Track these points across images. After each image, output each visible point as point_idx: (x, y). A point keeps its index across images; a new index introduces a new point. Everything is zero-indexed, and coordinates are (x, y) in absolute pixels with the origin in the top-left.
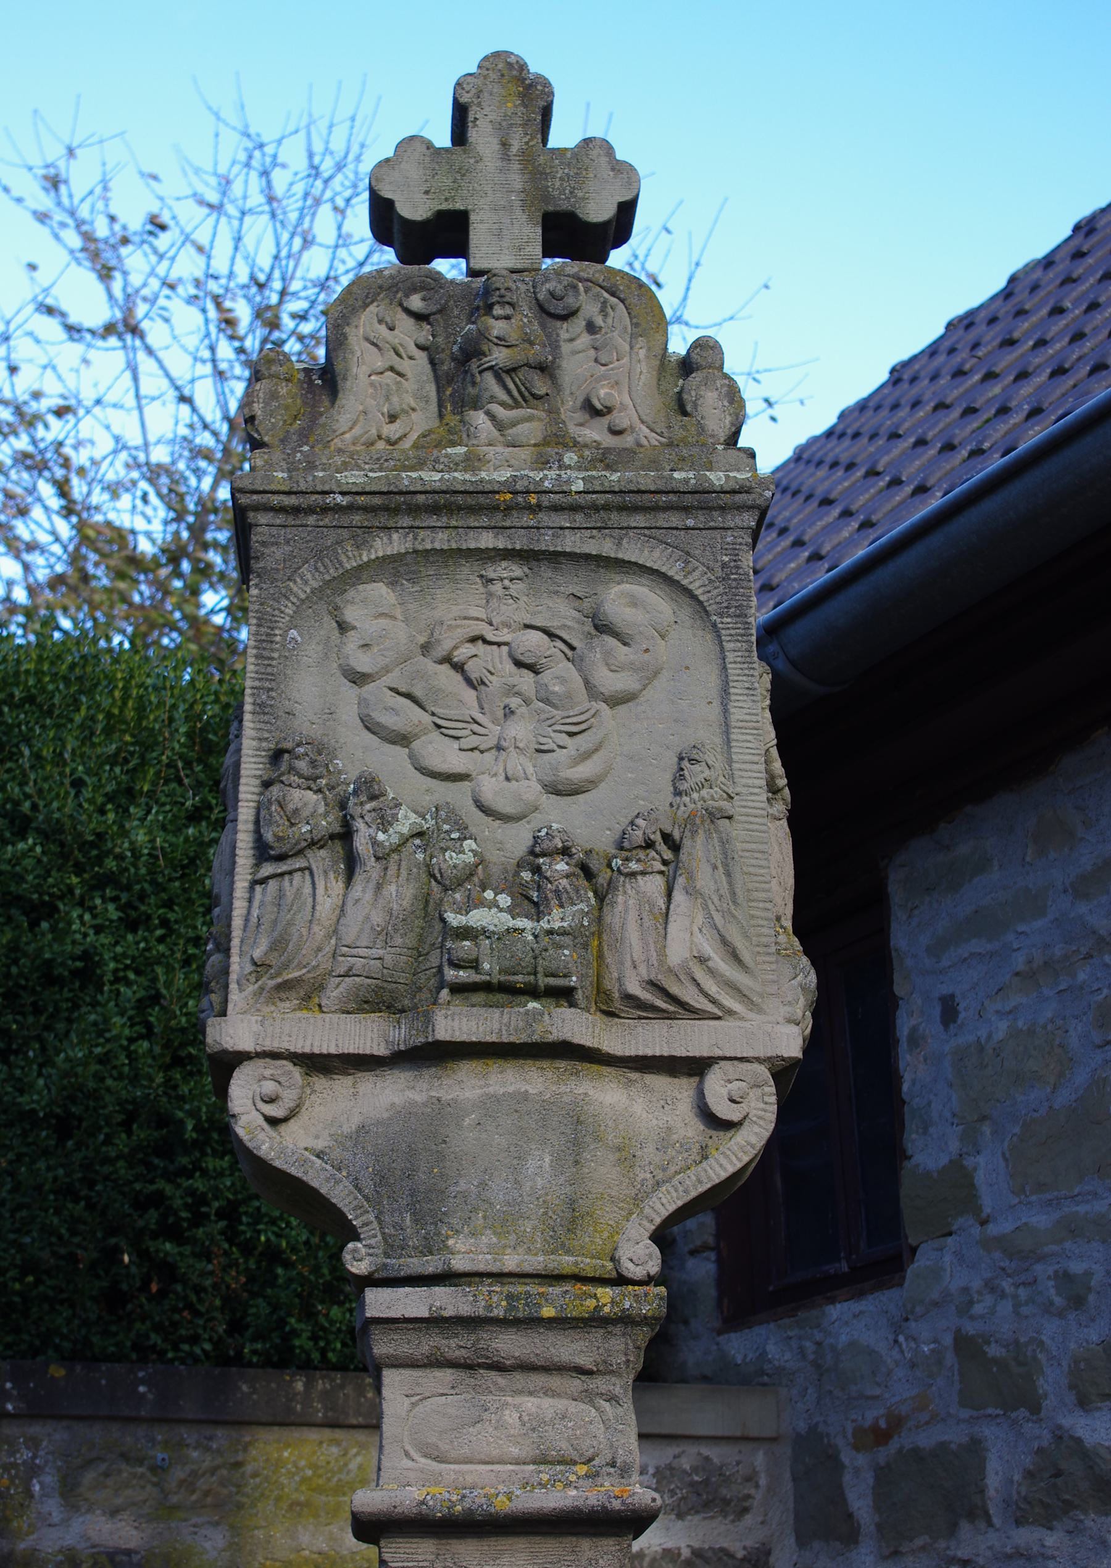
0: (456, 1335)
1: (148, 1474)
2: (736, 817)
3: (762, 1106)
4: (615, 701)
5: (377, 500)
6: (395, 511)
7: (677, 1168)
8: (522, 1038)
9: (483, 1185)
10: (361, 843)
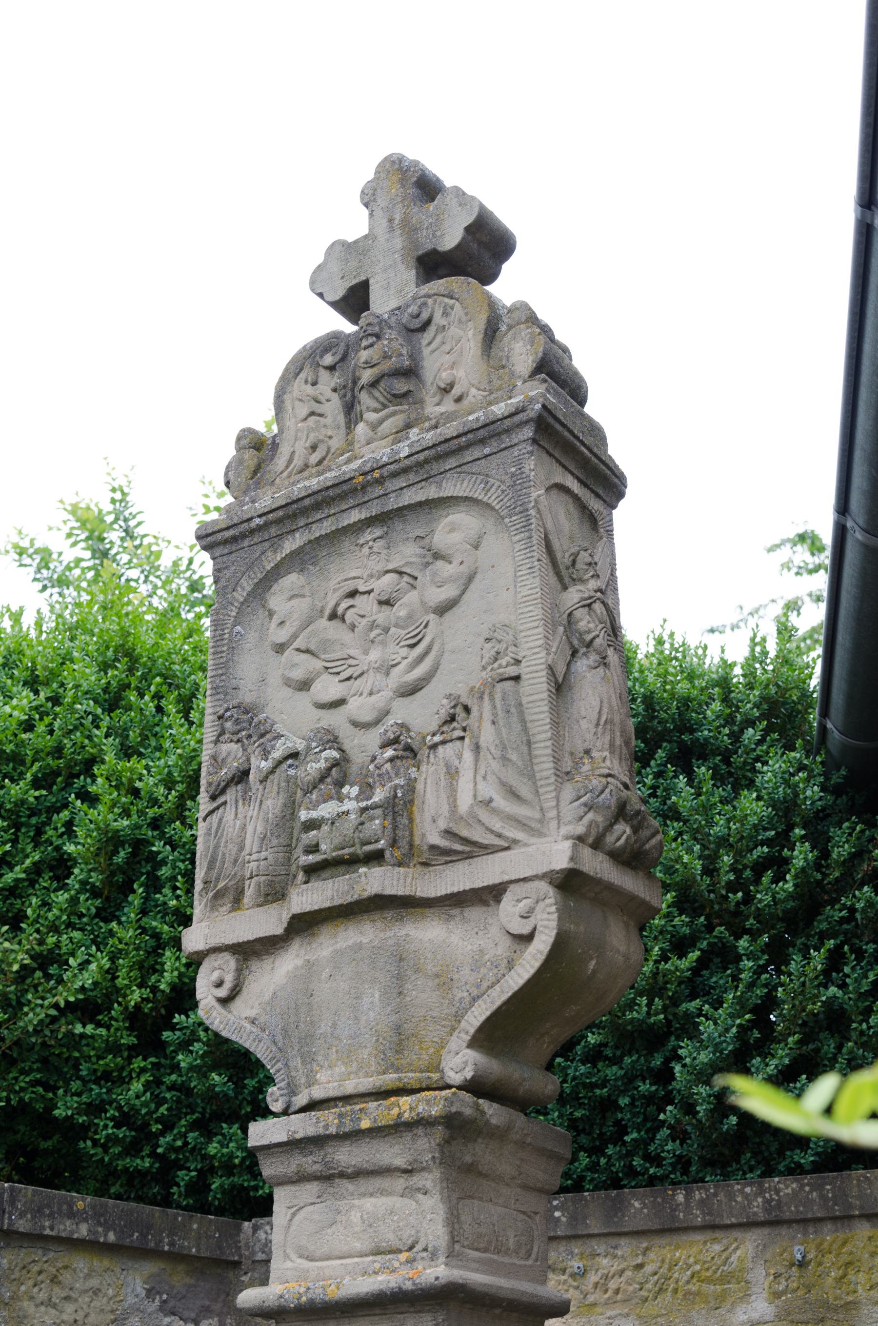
0: (311, 1153)
1: (570, 1280)
2: (524, 677)
3: (546, 916)
5: (280, 513)
6: (294, 516)
7: (489, 983)
9: (334, 1026)
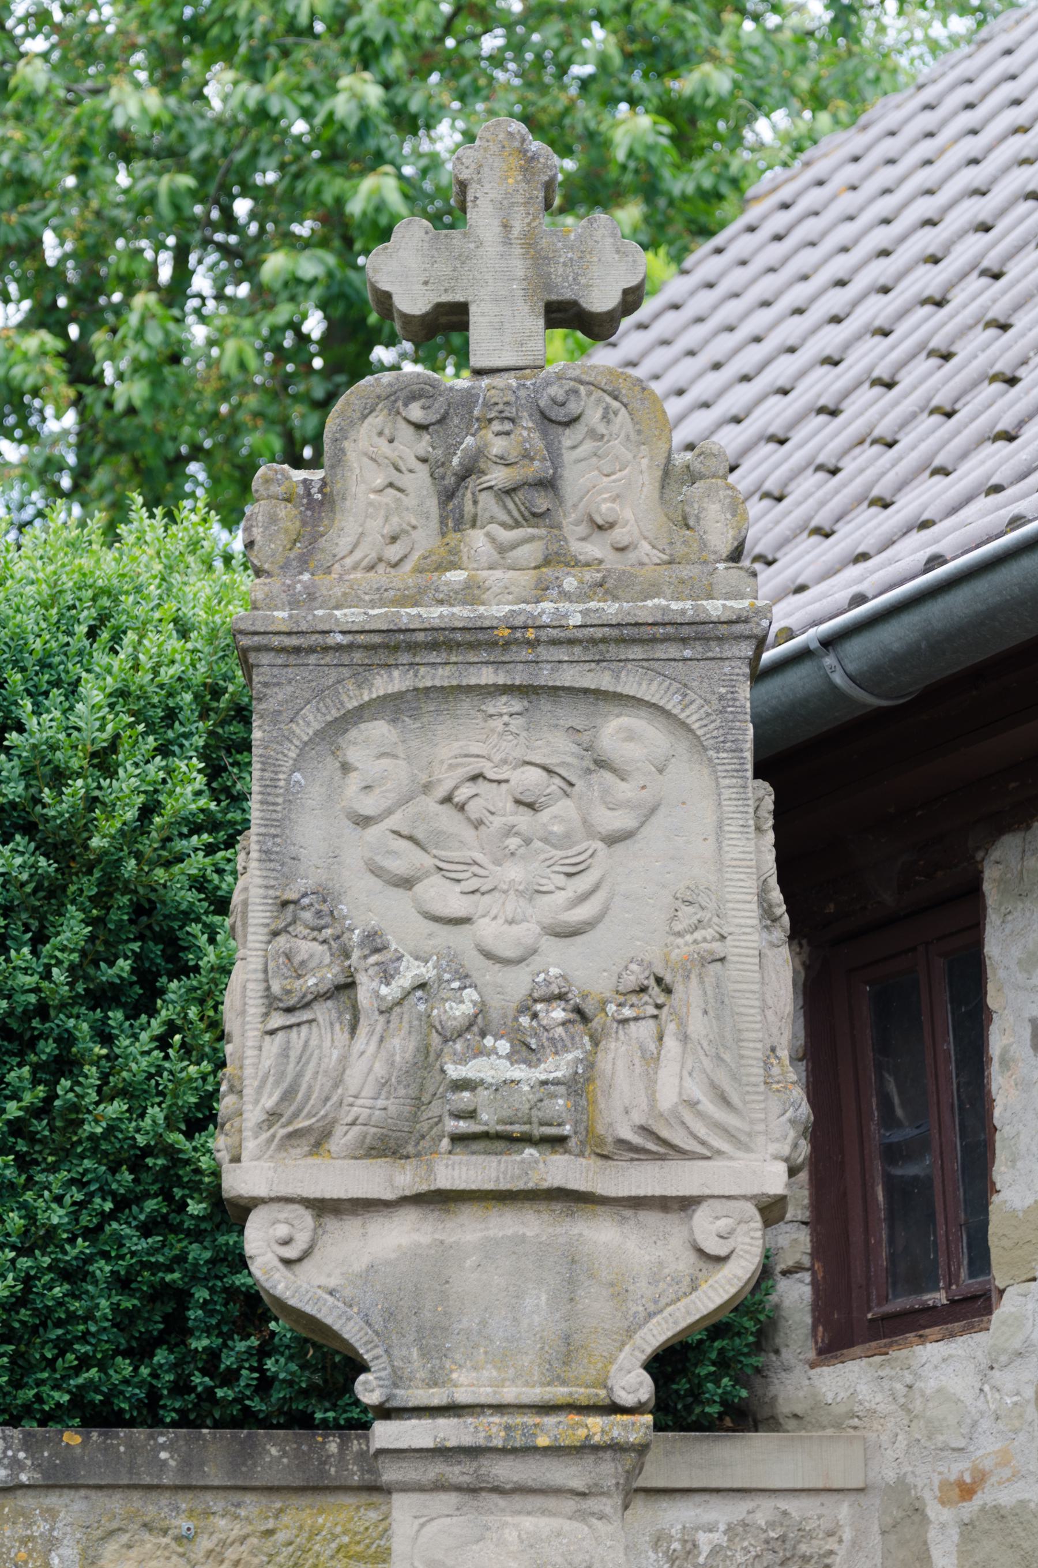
0: (460, 1463)
1: (173, 1545)
2: (729, 958)
3: (748, 1240)
4: (613, 840)
5: (377, 639)
6: (396, 648)
7: (668, 1300)
8: (520, 1185)
9: (483, 1323)
10: (363, 995)
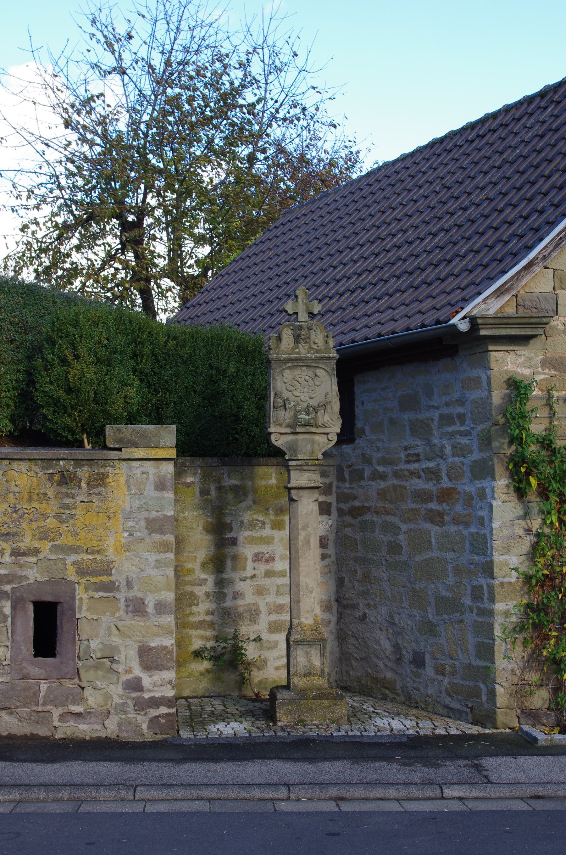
10: (287, 407)
